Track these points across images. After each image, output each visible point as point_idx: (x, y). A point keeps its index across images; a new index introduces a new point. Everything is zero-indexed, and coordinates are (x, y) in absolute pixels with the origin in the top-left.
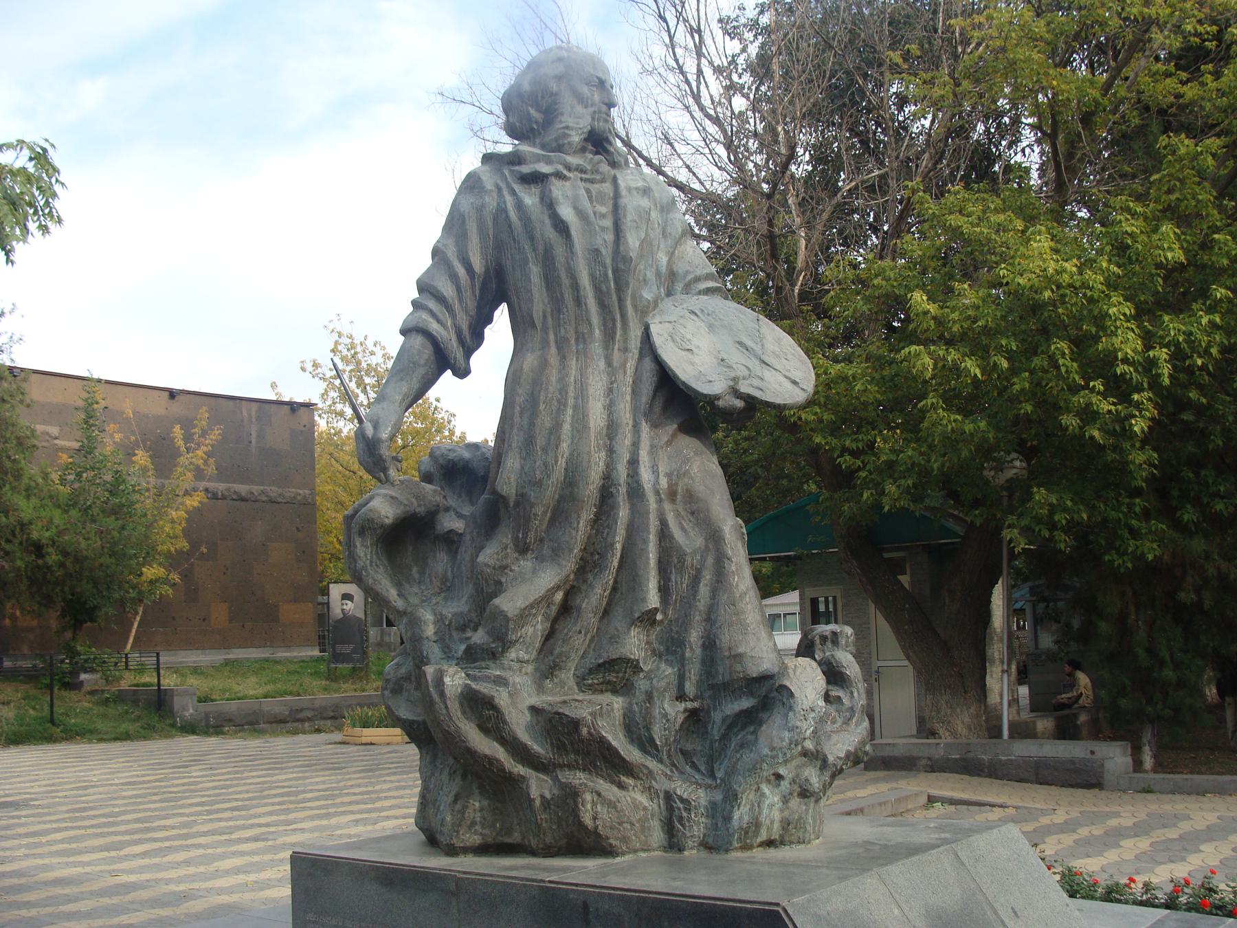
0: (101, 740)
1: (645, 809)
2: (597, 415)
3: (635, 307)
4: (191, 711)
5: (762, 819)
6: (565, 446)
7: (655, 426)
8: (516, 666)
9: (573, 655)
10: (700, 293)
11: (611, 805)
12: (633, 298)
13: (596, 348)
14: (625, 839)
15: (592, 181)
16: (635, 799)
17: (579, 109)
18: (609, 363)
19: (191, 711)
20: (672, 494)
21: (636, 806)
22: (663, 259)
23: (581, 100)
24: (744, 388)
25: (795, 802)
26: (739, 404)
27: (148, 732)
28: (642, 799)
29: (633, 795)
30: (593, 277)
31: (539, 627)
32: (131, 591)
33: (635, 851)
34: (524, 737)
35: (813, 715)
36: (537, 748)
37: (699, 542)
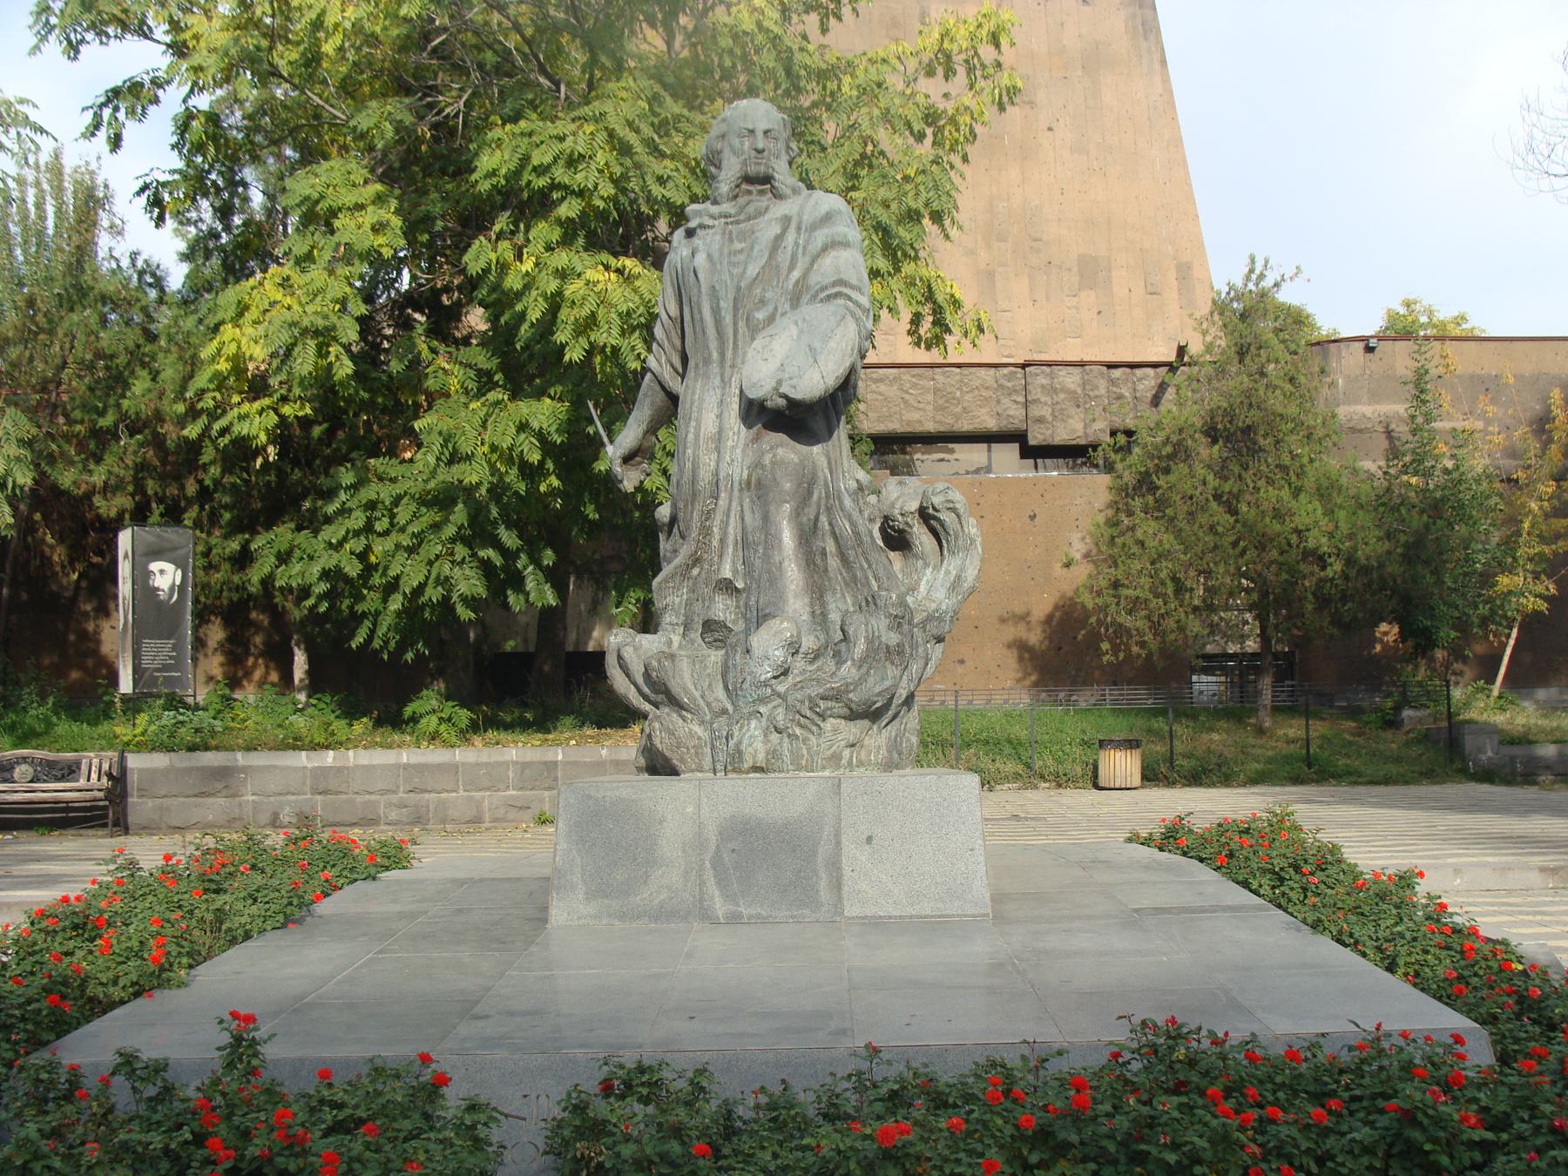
0: (1355, 783)
1: (699, 738)
2: (709, 424)
3: (748, 325)
4: (1490, 754)
5: (743, 747)
6: (689, 451)
7: (749, 427)
8: (670, 628)
9: (696, 619)
10: (822, 301)
11: (671, 733)
12: (748, 319)
13: (715, 368)
14: (682, 760)
15: (738, 222)
16: (690, 730)
17: (734, 160)
18: (722, 380)
19: (1490, 754)
20: (749, 483)
21: (691, 734)
22: (796, 274)
23: (736, 153)
24: (784, 389)
25: (775, 737)
26: (782, 402)
27: (1429, 775)
28: (698, 730)
29: (691, 726)
30: (712, 308)
31: (685, 597)
32: (1481, 606)
33: (692, 771)
34: (640, 680)
35: (768, 662)
36: (646, 690)
37: (759, 523)
